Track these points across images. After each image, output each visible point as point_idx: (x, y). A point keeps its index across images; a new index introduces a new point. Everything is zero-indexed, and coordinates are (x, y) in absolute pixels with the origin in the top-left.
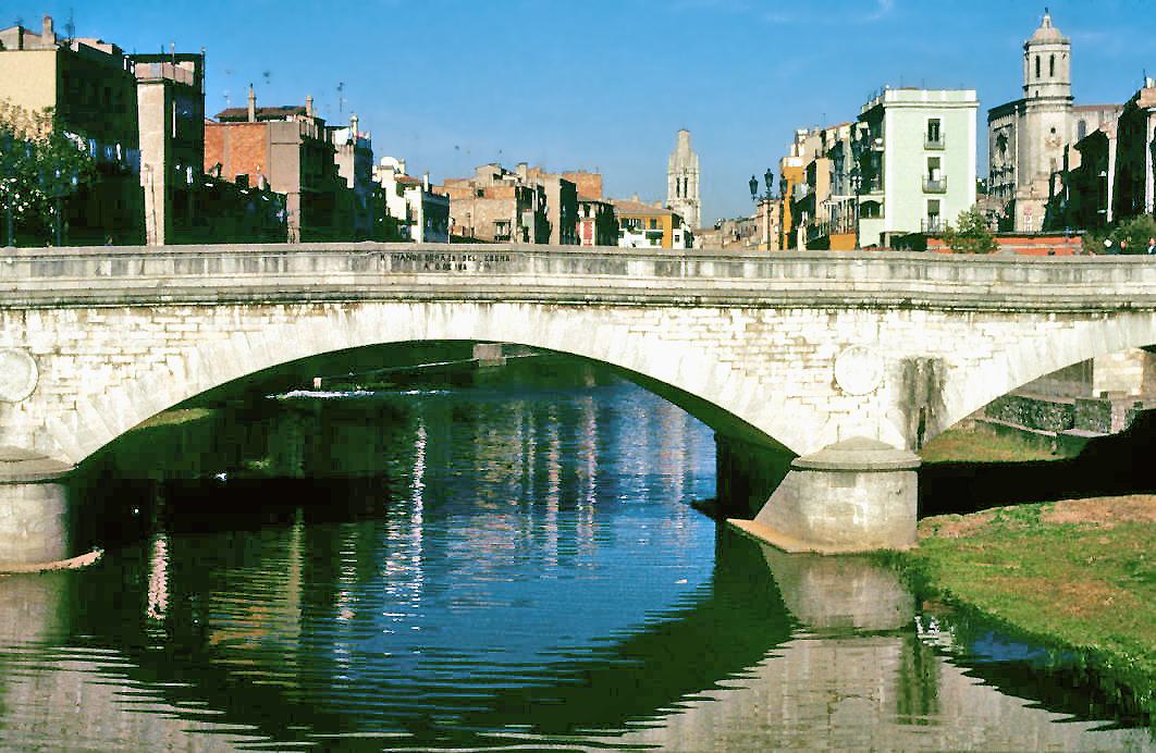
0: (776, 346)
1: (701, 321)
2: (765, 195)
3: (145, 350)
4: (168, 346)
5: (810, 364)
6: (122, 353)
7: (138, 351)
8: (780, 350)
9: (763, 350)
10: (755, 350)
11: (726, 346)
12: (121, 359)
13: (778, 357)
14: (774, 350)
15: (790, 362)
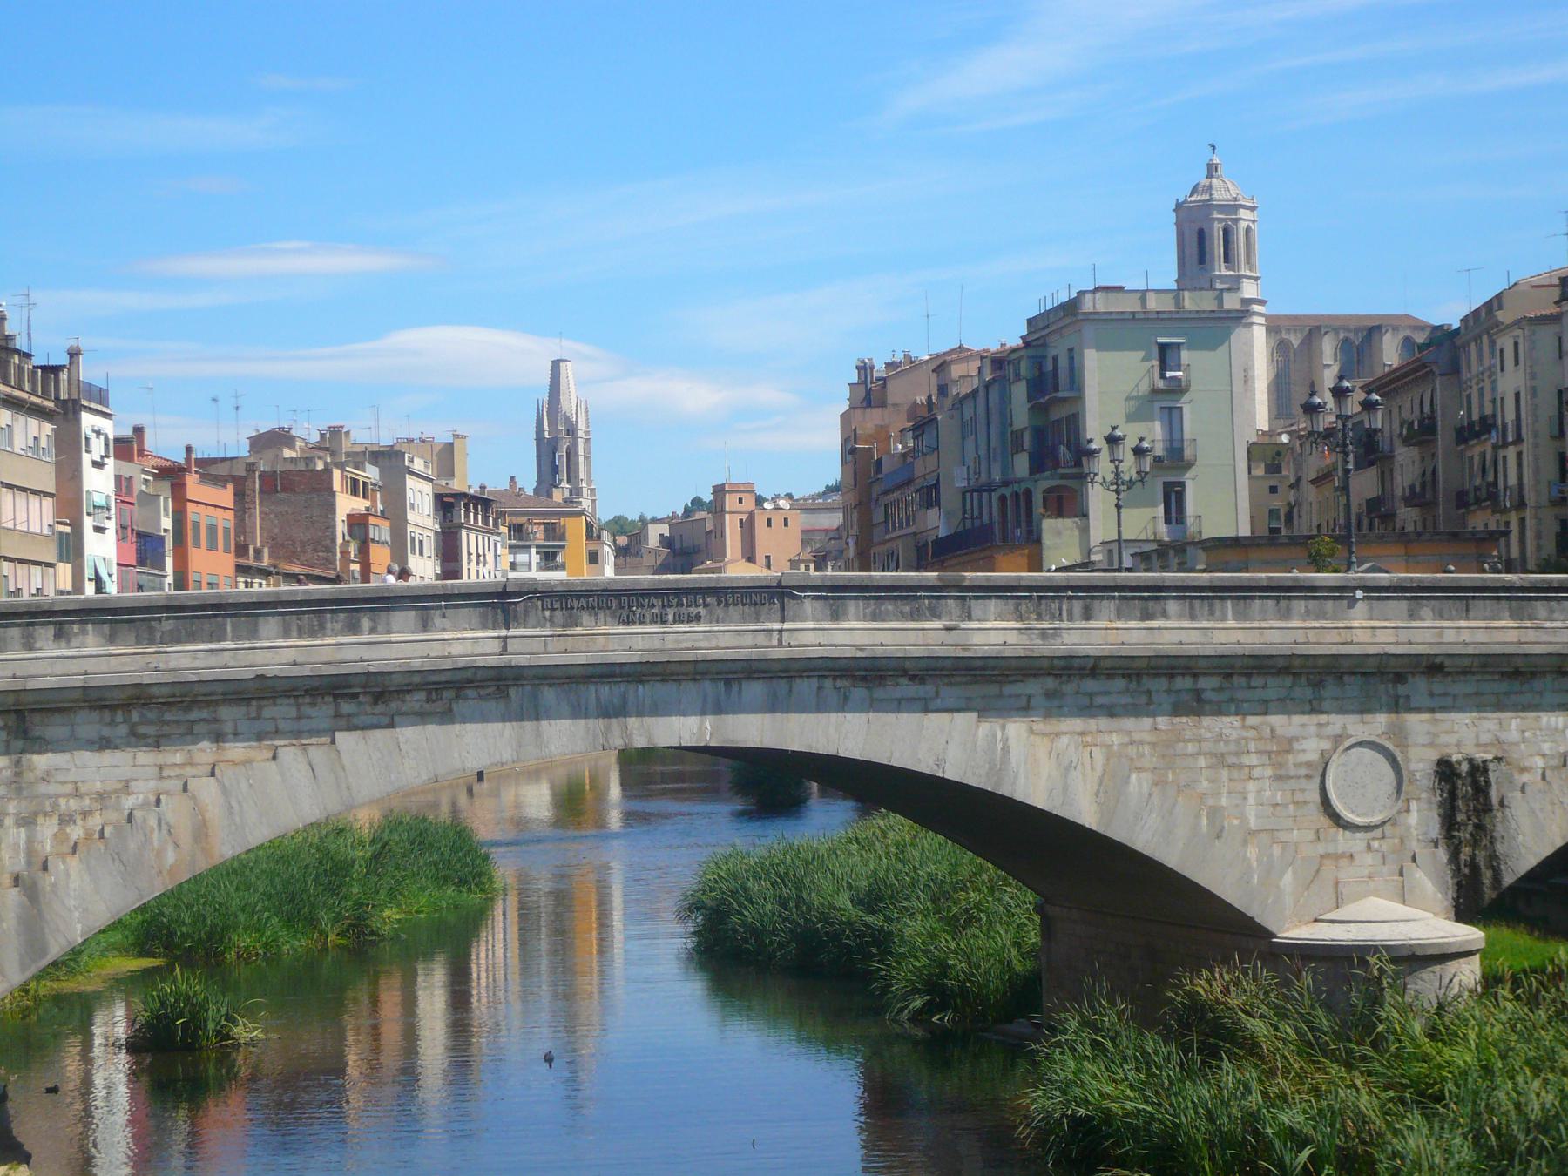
0: (1227, 742)
1: (1099, 700)
2: (1110, 477)
3: (119, 786)
4: (161, 778)
5: (1282, 772)
6: (77, 794)
7: (110, 786)
8: (1232, 747)
9: (1206, 747)
10: (1191, 748)
11: (1141, 743)
12: (74, 804)
13: (1231, 760)
14: (1222, 747)
15: (1252, 767)
